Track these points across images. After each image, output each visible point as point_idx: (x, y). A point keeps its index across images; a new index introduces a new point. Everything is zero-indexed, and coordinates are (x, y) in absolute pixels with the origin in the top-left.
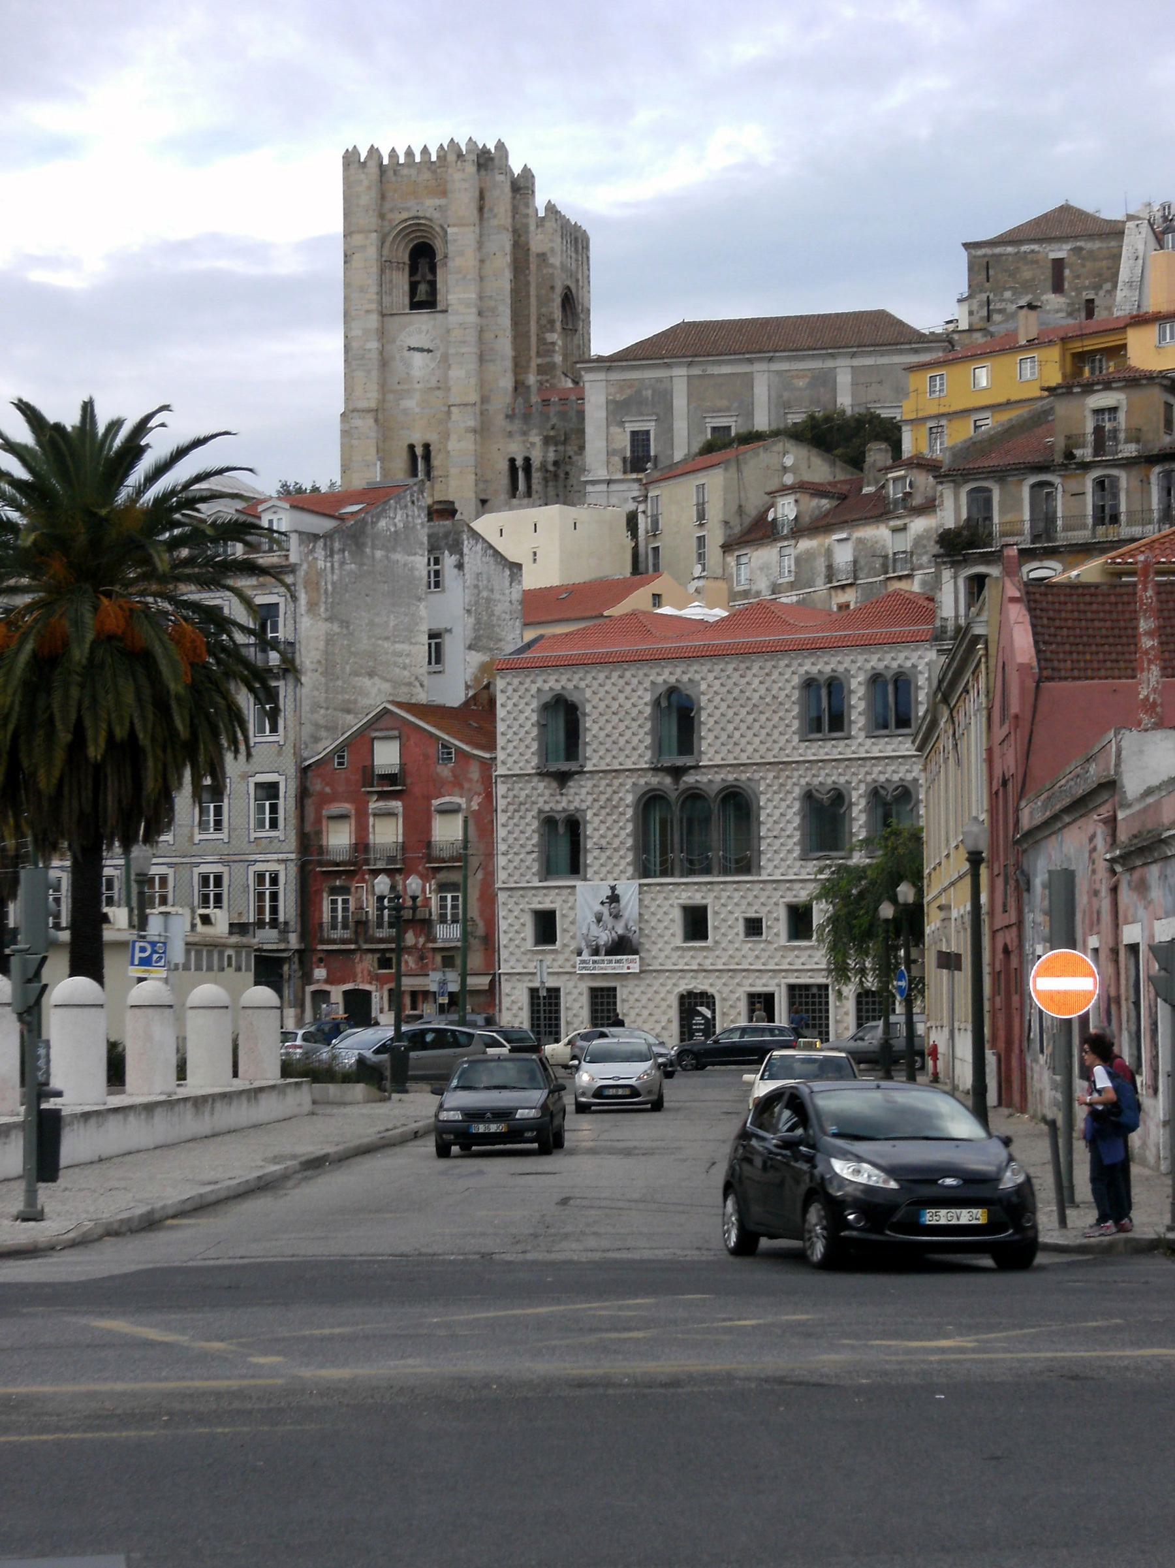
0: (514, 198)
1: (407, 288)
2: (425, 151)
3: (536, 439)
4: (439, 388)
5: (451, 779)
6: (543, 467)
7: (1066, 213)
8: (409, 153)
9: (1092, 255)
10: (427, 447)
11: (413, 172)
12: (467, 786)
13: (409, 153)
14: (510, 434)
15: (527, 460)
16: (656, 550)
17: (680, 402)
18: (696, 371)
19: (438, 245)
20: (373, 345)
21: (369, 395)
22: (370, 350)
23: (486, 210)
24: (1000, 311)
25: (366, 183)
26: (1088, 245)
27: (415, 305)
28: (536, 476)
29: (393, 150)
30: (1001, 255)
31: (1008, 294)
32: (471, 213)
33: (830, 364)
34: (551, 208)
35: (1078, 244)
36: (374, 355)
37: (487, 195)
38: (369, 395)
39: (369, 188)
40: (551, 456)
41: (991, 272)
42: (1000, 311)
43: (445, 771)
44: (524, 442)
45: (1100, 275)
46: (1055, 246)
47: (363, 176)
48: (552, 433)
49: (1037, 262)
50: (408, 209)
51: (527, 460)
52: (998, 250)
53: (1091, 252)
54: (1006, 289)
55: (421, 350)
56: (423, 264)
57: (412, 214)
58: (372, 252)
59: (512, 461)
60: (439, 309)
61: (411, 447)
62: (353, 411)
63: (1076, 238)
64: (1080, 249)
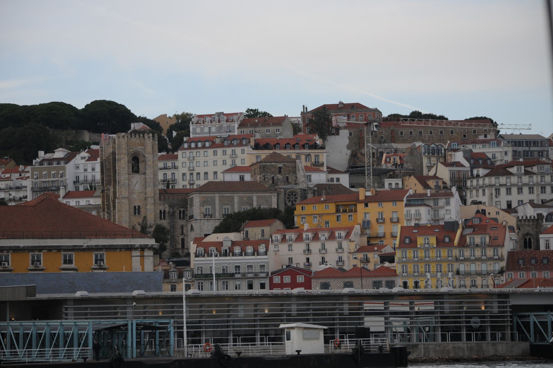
3: (167, 206)
4: (142, 193)
10: (139, 206)
14: (160, 204)
15: (164, 211)
17: (217, 202)
18: (221, 195)
20: (127, 182)
22: (126, 183)
24: (267, 178)
25: (124, 142)
26: (287, 164)
28: (167, 215)
31: (269, 174)
32: (151, 151)
33: (251, 195)
35: (285, 164)
36: (127, 184)
39: (125, 144)
40: (171, 210)
41: (265, 169)
42: (267, 178)
46: (279, 164)
47: (123, 141)
48: (171, 205)
49: (275, 167)
50: (133, 149)
51: (164, 211)
52: (266, 164)
60: (140, 173)
61: (135, 207)
63: (284, 162)
64: (285, 165)
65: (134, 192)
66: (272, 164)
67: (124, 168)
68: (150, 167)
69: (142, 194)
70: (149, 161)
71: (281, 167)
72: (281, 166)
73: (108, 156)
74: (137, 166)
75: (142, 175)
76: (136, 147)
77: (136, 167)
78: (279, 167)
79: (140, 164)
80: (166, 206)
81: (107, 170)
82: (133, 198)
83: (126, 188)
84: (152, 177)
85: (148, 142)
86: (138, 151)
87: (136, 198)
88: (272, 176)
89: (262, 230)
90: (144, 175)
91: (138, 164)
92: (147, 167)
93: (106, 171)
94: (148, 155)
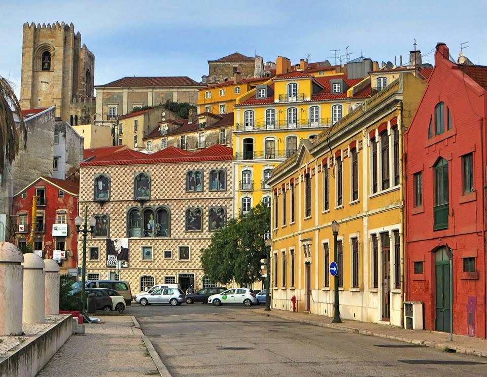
0: (75, 41)
1: (41, 64)
2: (49, 24)
3: (80, 110)
4: (50, 94)
5: (63, 203)
6: (81, 118)
7: (236, 54)
8: (44, 25)
9: (245, 67)
11: (45, 31)
12: (68, 205)
13: (44, 25)
15: (76, 116)
16: (121, 140)
17: (125, 100)
18: (130, 91)
19: (52, 52)
20: (30, 80)
23: (67, 42)
24: (218, 81)
25: (30, 33)
27: (44, 69)
29: (39, 24)
30: (219, 65)
31: (221, 76)
33: (171, 90)
34: (85, 46)
36: (31, 83)
37: (67, 38)
39: (31, 34)
40: (84, 115)
41: (216, 70)
43: (61, 200)
44: (76, 111)
45: (247, 72)
46: (235, 63)
48: (84, 108)
49: (229, 67)
51: (76, 116)
52: (218, 64)
53: (245, 66)
54: (221, 75)
55: (45, 83)
56: (47, 58)
57: (44, 43)
58: (31, 53)
59: (72, 116)
60: (51, 70)
62: (23, 99)
63: (241, 61)
64: (242, 64)
66: (225, 63)
69: (50, 95)
70: (59, 55)
71: (236, 67)
72: (236, 66)
78: (234, 67)
80: (78, 110)
83: (28, 88)
88: (225, 79)
89: (135, 121)
91: (50, 60)
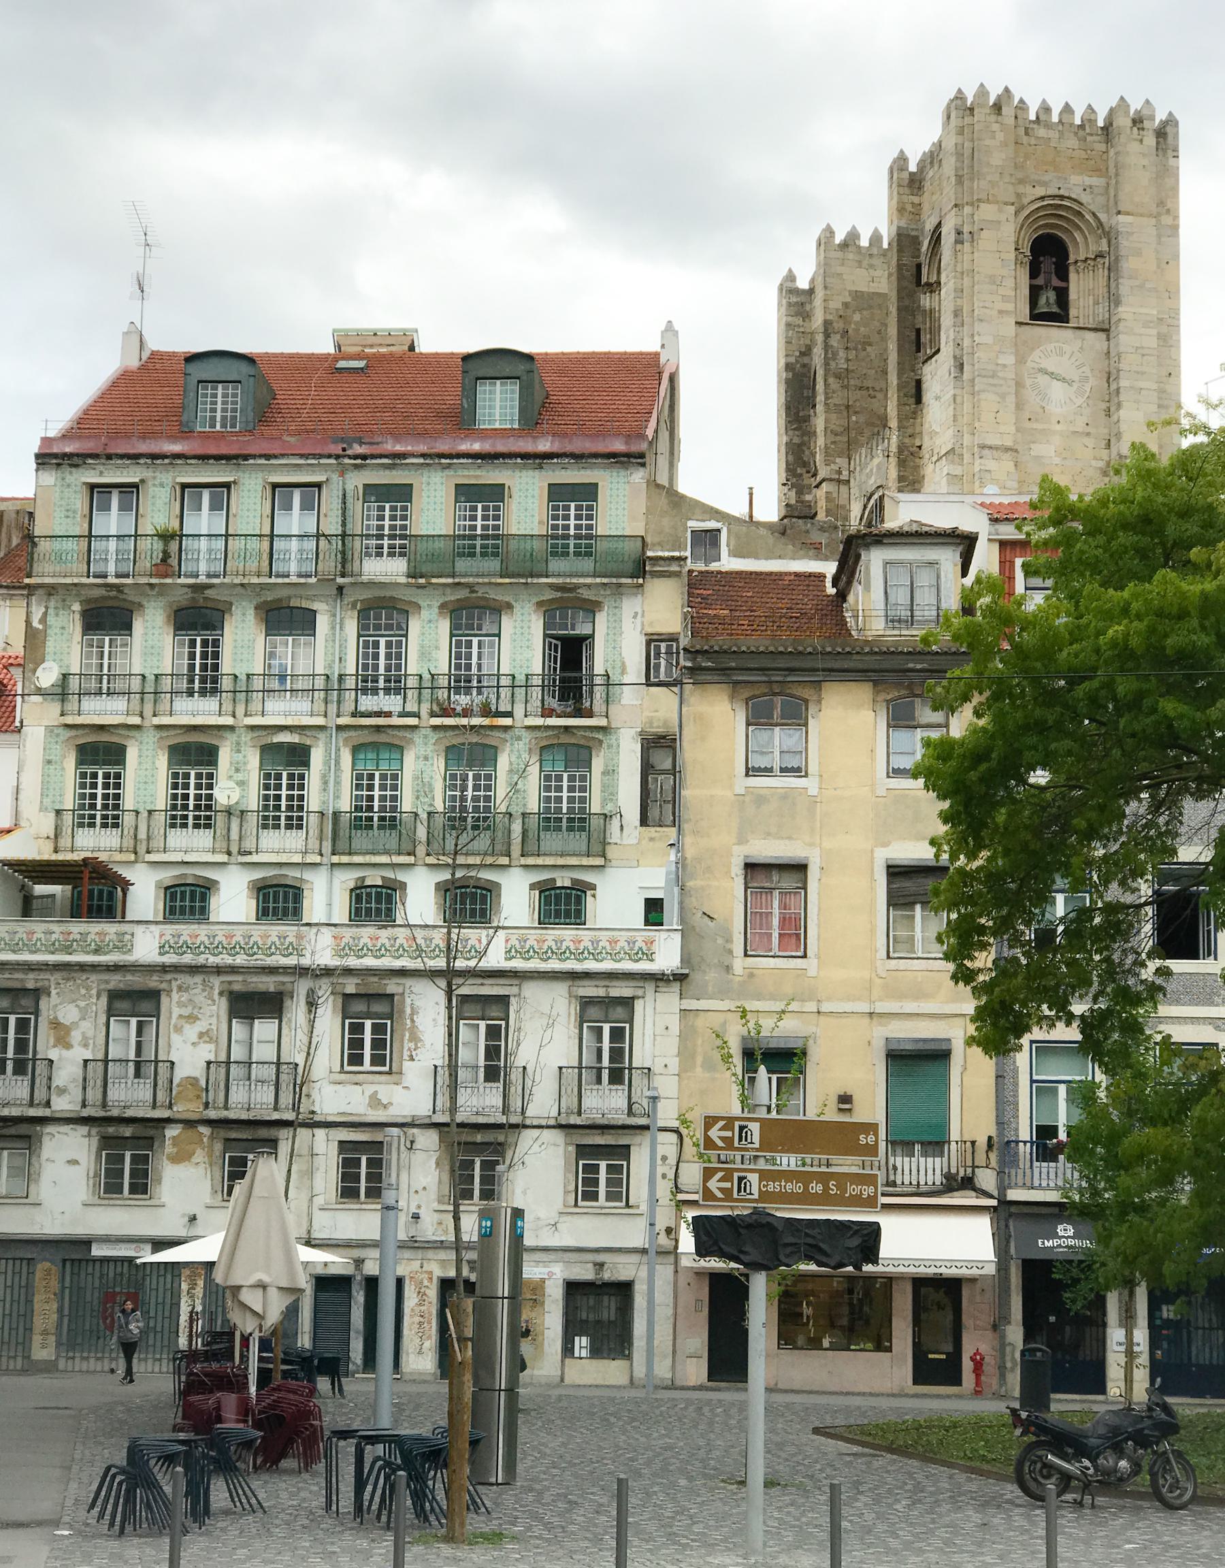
4: (1088, 434)
11: (1053, 134)
20: (1010, 360)
21: (1002, 428)
22: (1005, 366)
25: (1000, 136)
27: (1038, 316)
38: (1002, 428)
39: (1005, 144)
47: (996, 127)
50: (1044, 184)
65: (1039, 426)
67: (992, 280)
68: (1141, 286)
69: (1087, 441)
70: (1138, 253)
73: (846, 305)
74: (1055, 289)
75: (1090, 335)
76: (1059, 178)
77: (1052, 296)
79: (1073, 276)
81: (838, 376)
82: (1037, 458)
83: (1003, 396)
84: (1153, 343)
85: (1134, 147)
86: (1069, 198)
87: (1057, 460)
90: (1103, 335)
91: (1063, 275)
92: (1125, 286)
93: (831, 380)
94: (1129, 219)
